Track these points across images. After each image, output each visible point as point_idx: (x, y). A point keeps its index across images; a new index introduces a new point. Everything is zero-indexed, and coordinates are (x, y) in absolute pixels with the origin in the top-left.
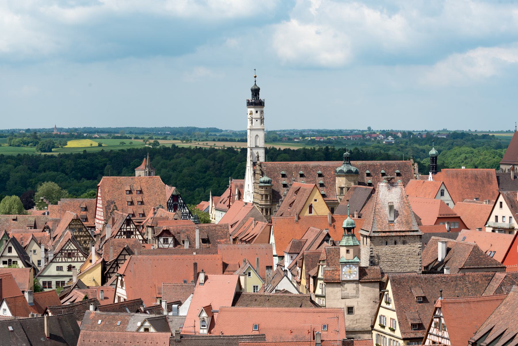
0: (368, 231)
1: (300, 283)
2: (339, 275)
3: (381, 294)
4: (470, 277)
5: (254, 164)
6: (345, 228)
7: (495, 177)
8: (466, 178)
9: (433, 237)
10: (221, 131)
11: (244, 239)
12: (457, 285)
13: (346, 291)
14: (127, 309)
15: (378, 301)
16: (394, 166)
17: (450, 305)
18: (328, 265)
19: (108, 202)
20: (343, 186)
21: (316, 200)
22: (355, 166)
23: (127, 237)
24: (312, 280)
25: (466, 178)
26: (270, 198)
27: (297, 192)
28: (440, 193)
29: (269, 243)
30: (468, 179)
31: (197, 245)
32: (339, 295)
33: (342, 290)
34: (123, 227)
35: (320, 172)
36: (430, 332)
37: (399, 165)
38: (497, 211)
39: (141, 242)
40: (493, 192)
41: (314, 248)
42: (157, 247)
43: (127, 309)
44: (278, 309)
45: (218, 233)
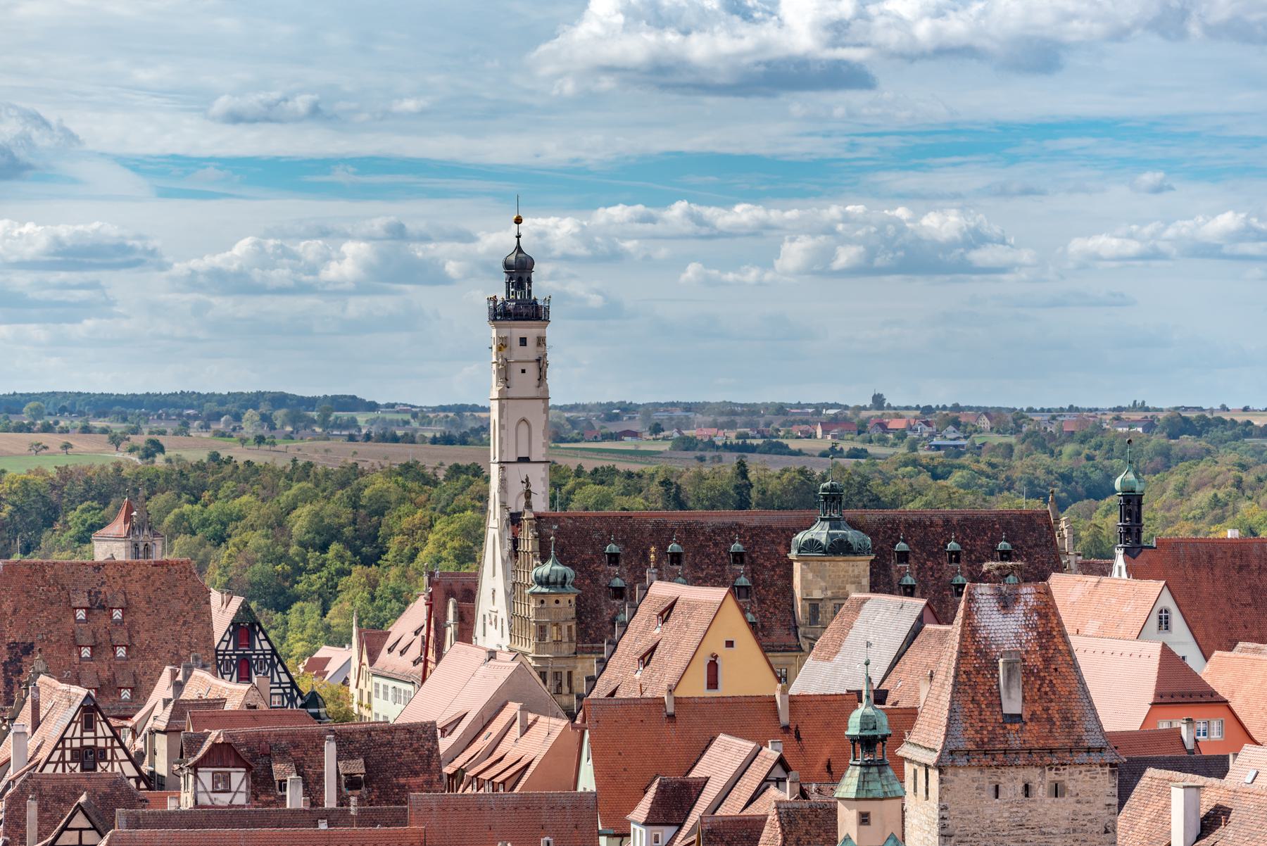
0: (934, 750)
6: (854, 740)
8: (1241, 568)
9: (1151, 772)
10: (373, 406)
16: (993, 529)
20: (817, 594)
21: (730, 644)
22: (859, 529)
23: (83, 769)
25: (1241, 568)
26: (570, 636)
27: (666, 613)
29: (576, 788)
30: (1251, 572)
31: (330, 800)
34: (69, 734)
35: (736, 547)
37: (1009, 523)
39: (132, 782)
42: (191, 804)
45: (399, 755)
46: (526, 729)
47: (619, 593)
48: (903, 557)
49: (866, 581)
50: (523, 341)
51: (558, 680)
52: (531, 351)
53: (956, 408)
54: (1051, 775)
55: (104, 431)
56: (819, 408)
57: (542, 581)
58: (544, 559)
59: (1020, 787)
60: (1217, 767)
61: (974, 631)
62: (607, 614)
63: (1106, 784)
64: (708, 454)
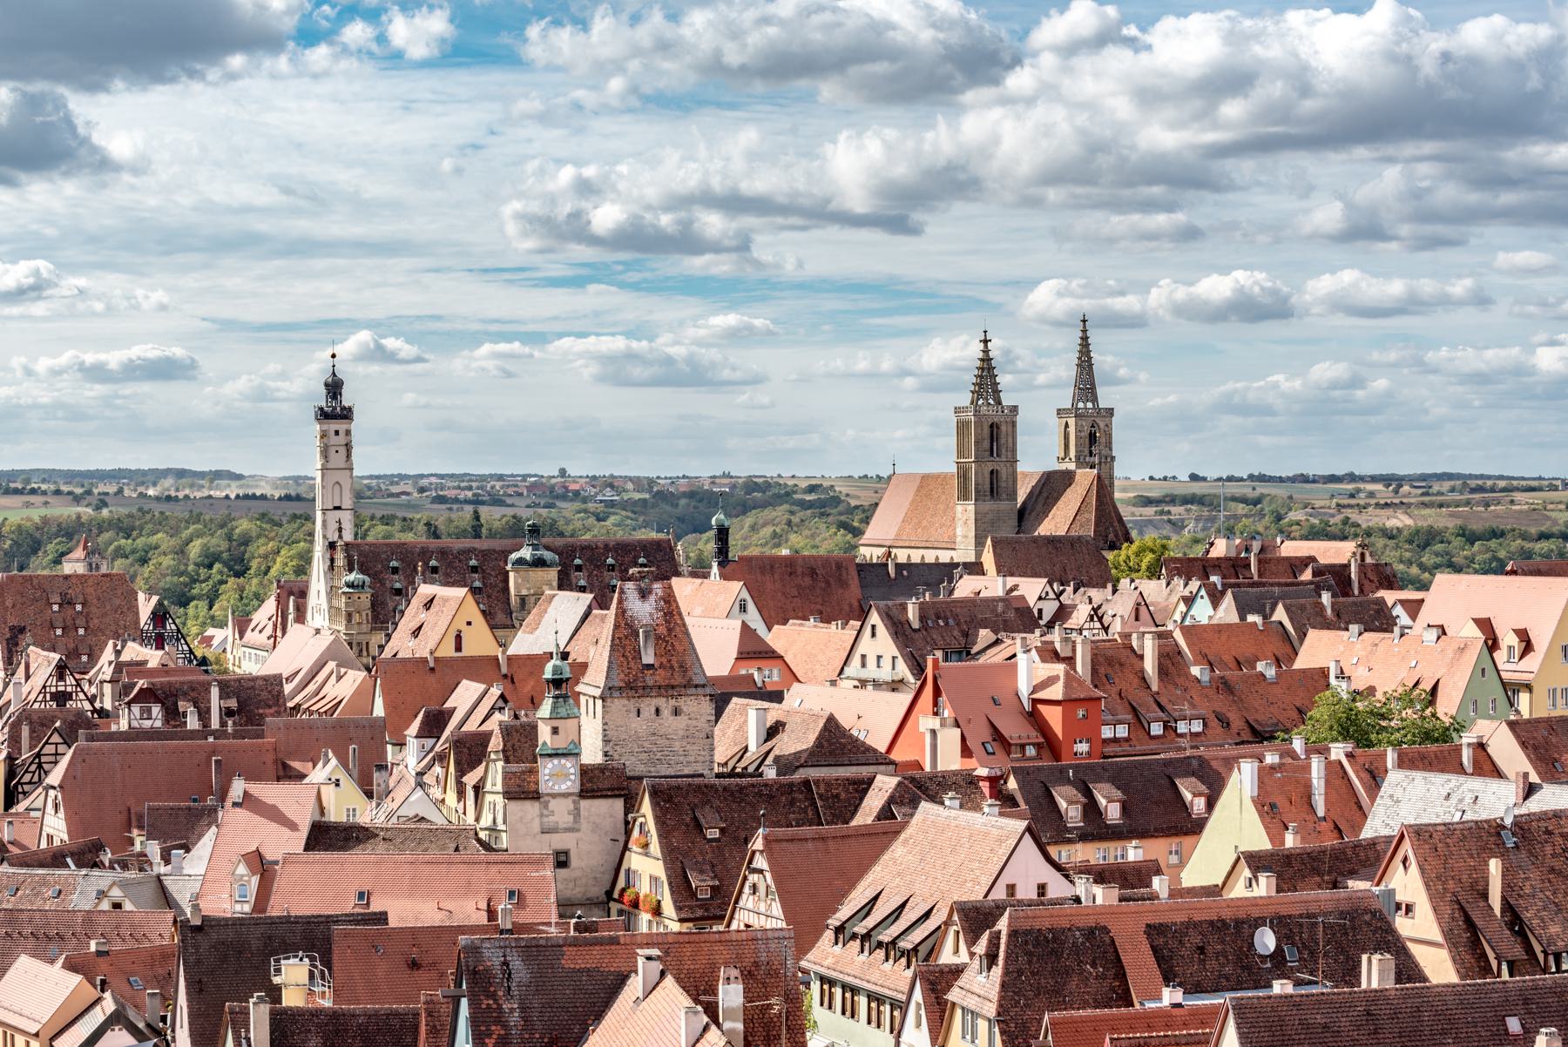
1: (443, 801)
2: (537, 783)
3: (627, 823)
4: (822, 786)
5: (332, 546)
6: (548, 681)
7: (853, 572)
9: (735, 700)
10: (239, 477)
11: (314, 708)
12: (792, 803)
13: (551, 818)
14: (69, 860)
15: (622, 839)
17: (784, 844)
18: (507, 761)
19: (12, 629)
20: (524, 592)
21: (469, 623)
24: (470, 794)
27: (428, 605)
28: (737, 606)
31: (215, 723)
32: (536, 826)
33: (542, 815)
35: (473, 562)
36: (741, 904)
38: (866, 645)
40: (851, 606)
41: (472, 726)
43: (69, 860)
44: (408, 856)
46: (339, 678)
47: (398, 592)
48: (579, 568)
49: (555, 584)
50: (337, 433)
51: (361, 648)
52: (342, 439)
53: (612, 476)
54: (673, 702)
55: (70, 493)
56: (525, 477)
57: (350, 585)
58: (351, 570)
59: (653, 710)
60: (777, 697)
61: (624, 612)
62: (391, 605)
63: (707, 708)
64: (455, 507)
